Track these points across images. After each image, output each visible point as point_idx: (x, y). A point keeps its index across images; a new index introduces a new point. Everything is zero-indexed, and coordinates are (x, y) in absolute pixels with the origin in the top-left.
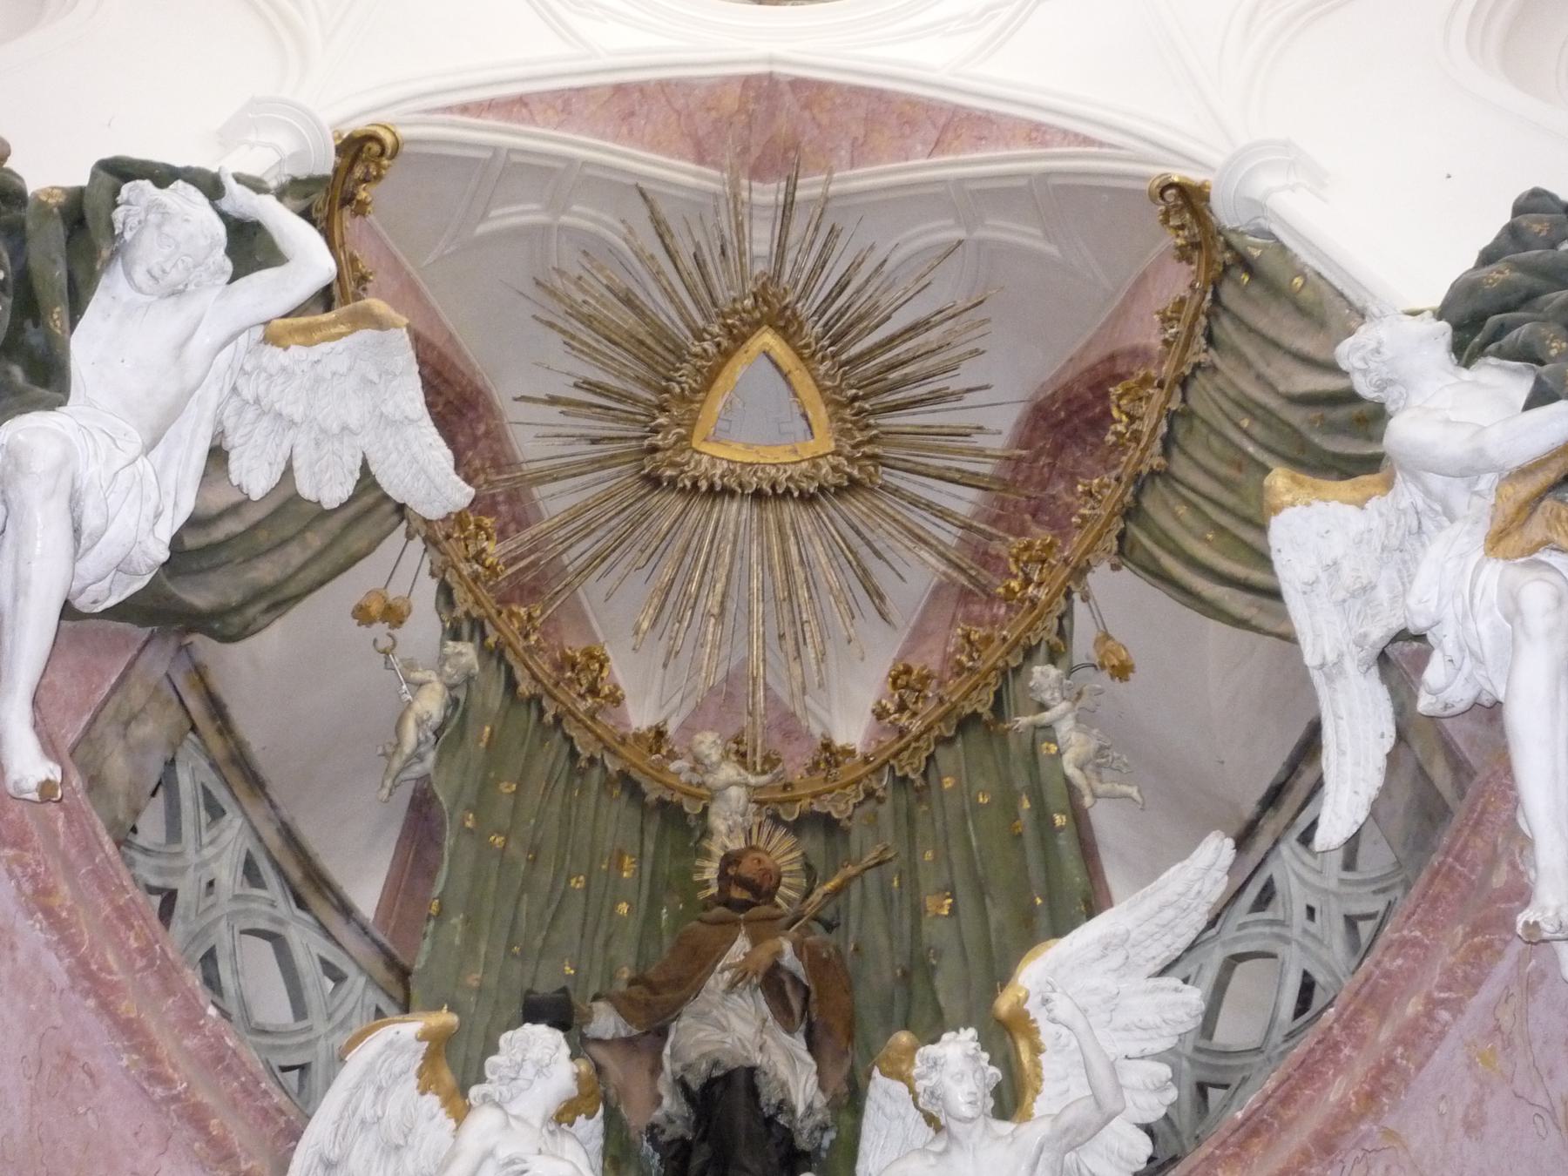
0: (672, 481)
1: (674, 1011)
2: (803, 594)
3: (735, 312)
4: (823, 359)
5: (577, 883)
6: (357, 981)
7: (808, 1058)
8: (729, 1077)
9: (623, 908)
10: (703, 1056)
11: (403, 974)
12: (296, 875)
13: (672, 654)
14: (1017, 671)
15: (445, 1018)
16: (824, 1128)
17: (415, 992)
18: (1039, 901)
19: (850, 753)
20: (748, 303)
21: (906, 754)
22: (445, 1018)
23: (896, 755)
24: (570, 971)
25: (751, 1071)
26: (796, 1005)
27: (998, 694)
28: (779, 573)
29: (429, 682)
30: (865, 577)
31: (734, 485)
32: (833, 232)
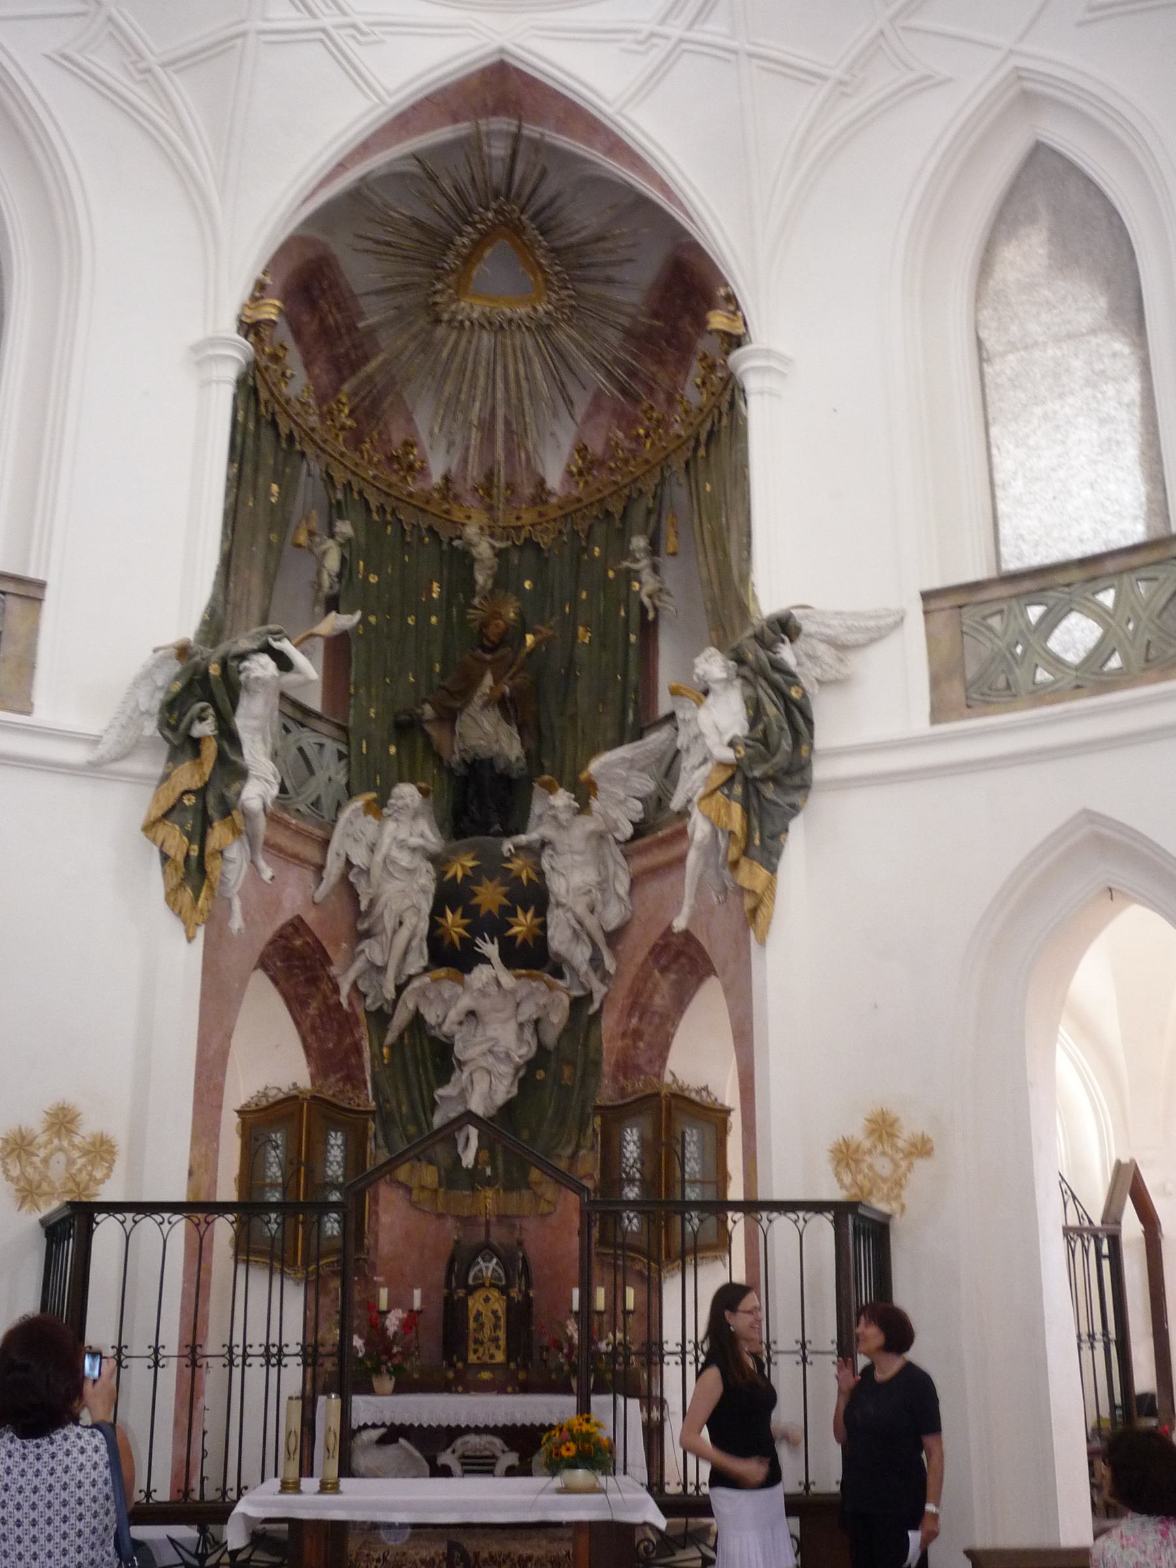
0: (450, 321)
1: (461, 710)
2: (527, 402)
3: (483, 221)
4: (540, 247)
5: (411, 621)
6: (328, 743)
7: (517, 736)
8: (482, 761)
9: (434, 620)
10: (472, 747)
11: (343, 729)
12: (299, 716)
13: (451, 444)
14: (635, 500)
15: (373, 795)
16: (522, 769)
17: (351, 737)
18: (619, 677)
19: (550, 493)
20: (490, 215)
21: (579, 515)
22: (373, 795)
23: (575, 512)
24: (412, 679)
25: (491, 759)
26: (512, 712)
27: (625, 508)
28: (513, 385)
29: (331, 547)
30: (562, 388)
31: (486, 325)
32: (544, 173)
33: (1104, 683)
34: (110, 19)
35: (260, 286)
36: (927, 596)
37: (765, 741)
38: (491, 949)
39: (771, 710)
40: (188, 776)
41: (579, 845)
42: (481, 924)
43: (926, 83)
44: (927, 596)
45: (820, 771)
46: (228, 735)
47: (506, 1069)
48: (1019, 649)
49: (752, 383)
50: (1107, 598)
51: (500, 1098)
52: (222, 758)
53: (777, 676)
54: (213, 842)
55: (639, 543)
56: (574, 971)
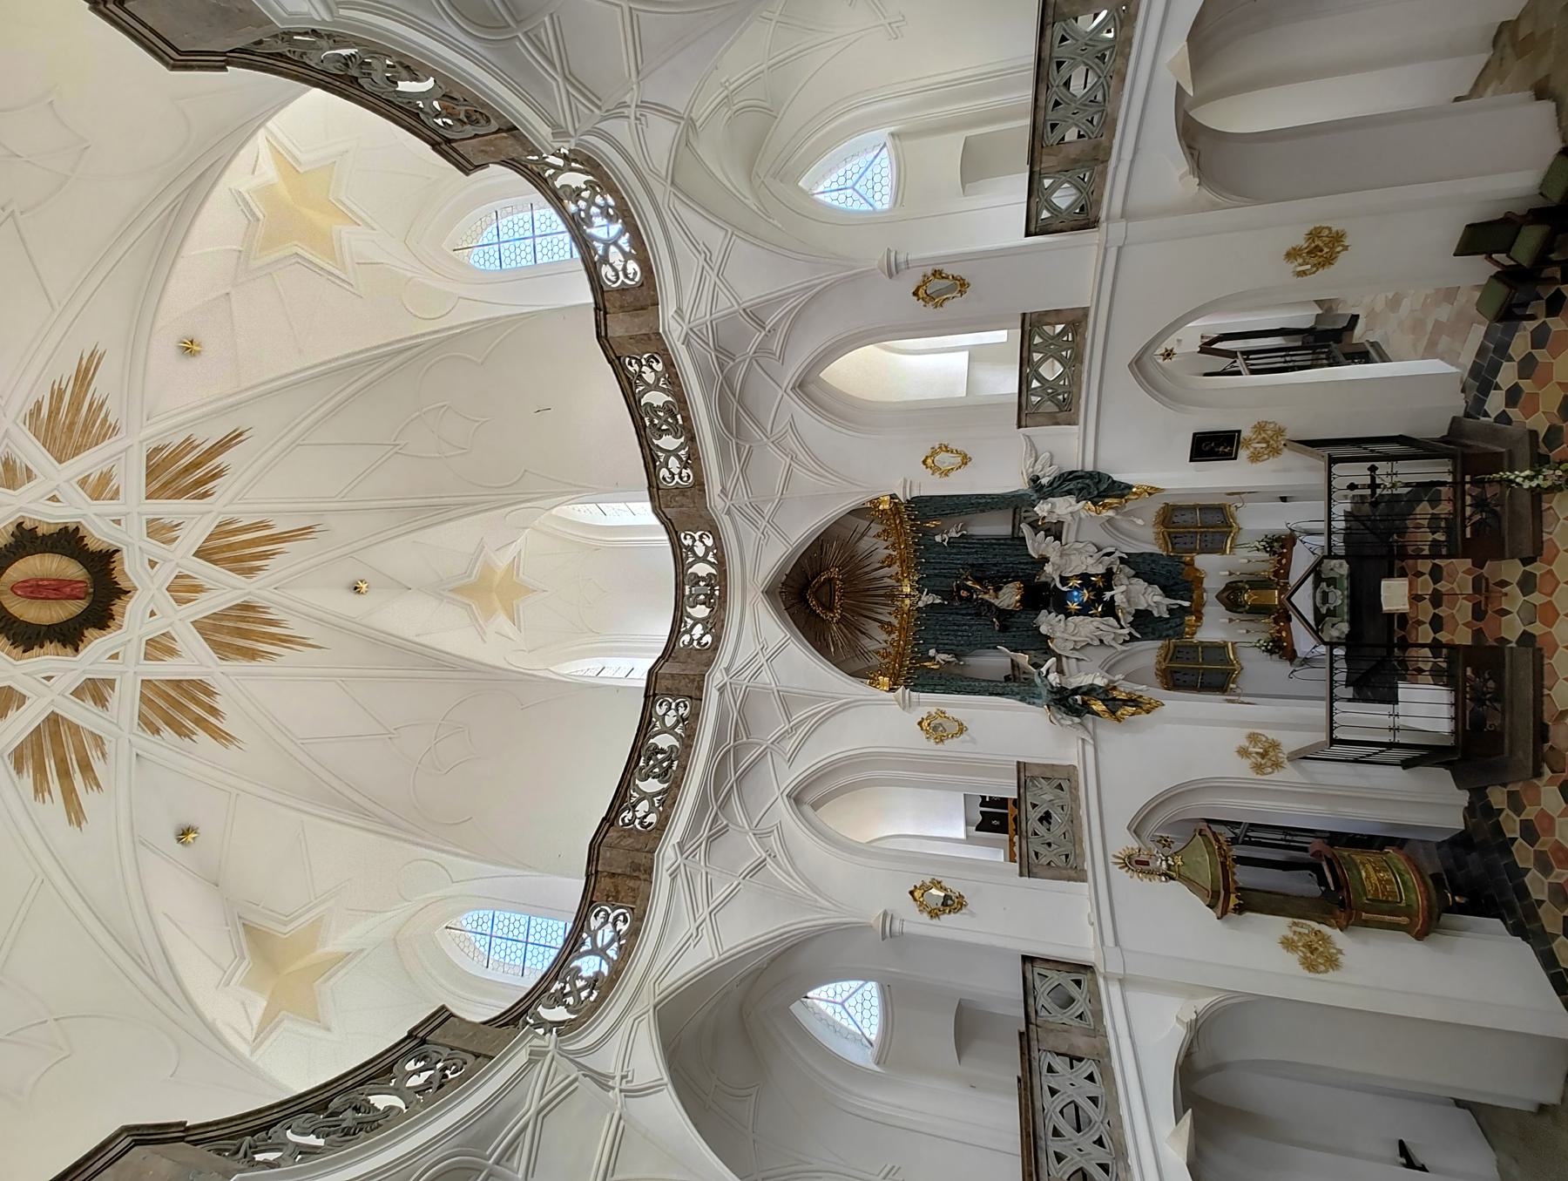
33: (1077, 358)
34: (772, 743)
35: (871, 684)
36: (1019, 426)
37: (1081, 490)
38: (1108, 595)
39: (1071, 486)
40: (1098, 706)
41: (1064, 561)
42: (1099, 599)
43: (792, 425)
44: (1019, 426)
45: (1089, 468)
46: (1076, 691)
47: (1150, 589)
48: (1050, 391)
49: (915, 494)
50: (1036, 357)
51: (1161, 592)
52: (1084, 694)
53: (1055, 485)
54: (1123, 696)
55: (938, 539)
56: (1112, 563)
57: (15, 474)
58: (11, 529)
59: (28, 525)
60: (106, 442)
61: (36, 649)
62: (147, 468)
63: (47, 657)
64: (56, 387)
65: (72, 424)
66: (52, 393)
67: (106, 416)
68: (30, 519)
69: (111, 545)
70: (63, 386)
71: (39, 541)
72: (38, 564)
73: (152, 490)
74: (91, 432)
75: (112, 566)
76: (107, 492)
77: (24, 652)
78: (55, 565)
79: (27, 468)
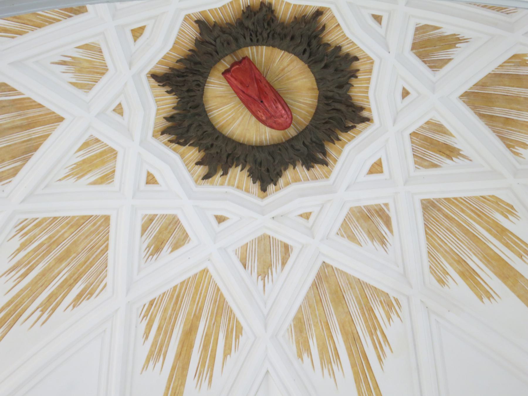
57: (160, 232)
58: (217, 178)
59: (202, 170)
60: (41, 216)
61: (346, 49)
62: (26, 160)
63: (348, 35)
64: (45, 316)
65: (60, 260)
66: (54, 310)
67: (19, 251)
68: (192, 175)
69: (152, 87)
70: (38, 313)
71: (213, 151)
72: (238, 122)
73: (46, 127)
74: (50, 238)
75: (178, 66)
76: (96, 149)
77: (356, 59)
78: (226, 108)
79: (144, 230)
